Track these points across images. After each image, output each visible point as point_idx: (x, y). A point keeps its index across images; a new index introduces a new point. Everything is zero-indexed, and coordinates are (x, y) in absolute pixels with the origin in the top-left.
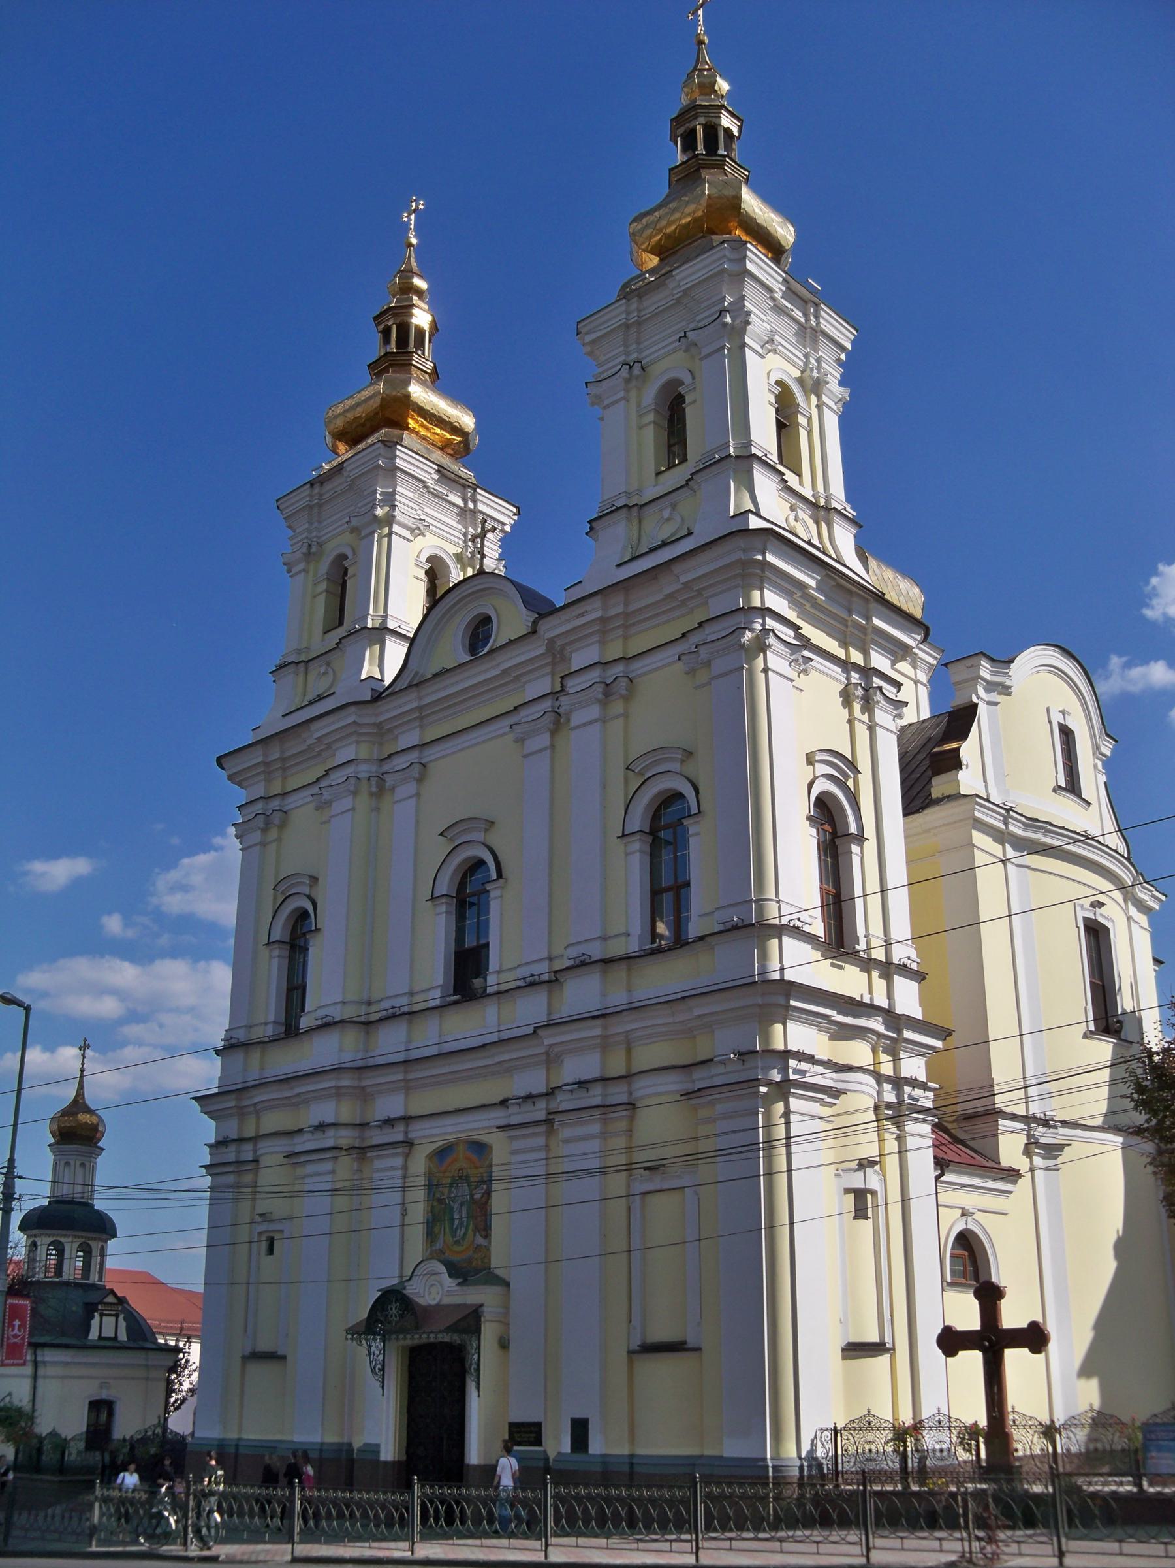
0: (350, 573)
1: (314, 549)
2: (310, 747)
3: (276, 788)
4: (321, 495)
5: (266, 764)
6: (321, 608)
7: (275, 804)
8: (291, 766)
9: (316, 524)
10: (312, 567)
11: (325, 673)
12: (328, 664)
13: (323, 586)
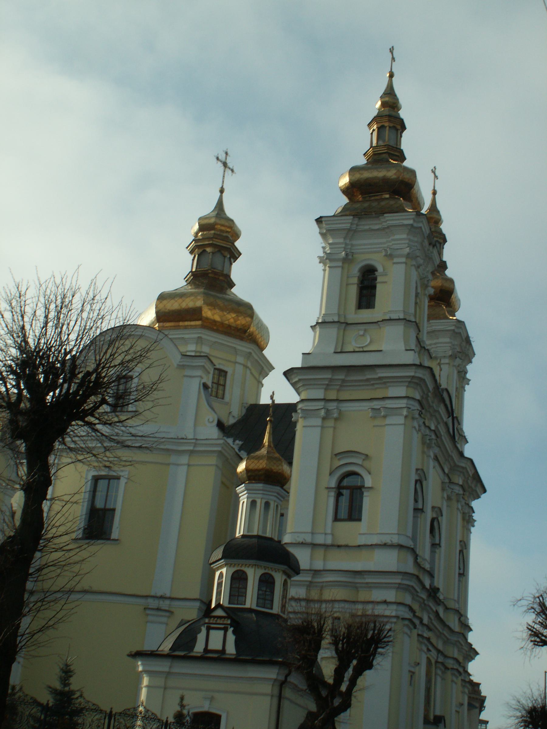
0: (379, 279)
1: (350, 257)
2: (368, 380)
3: (332, 395)
4: (357, 225)
5: (331, 380)
6: (353, 291)
7: (332, 406)
8: (347, 386)
9: (348, 241)
10: (346, 266)
11: (363, 335)
12: (365, 330)
13: (355, 280)
